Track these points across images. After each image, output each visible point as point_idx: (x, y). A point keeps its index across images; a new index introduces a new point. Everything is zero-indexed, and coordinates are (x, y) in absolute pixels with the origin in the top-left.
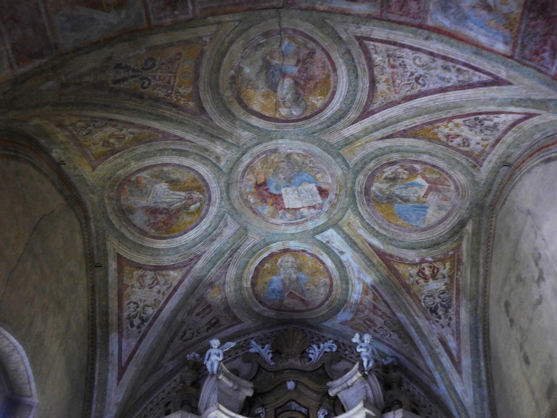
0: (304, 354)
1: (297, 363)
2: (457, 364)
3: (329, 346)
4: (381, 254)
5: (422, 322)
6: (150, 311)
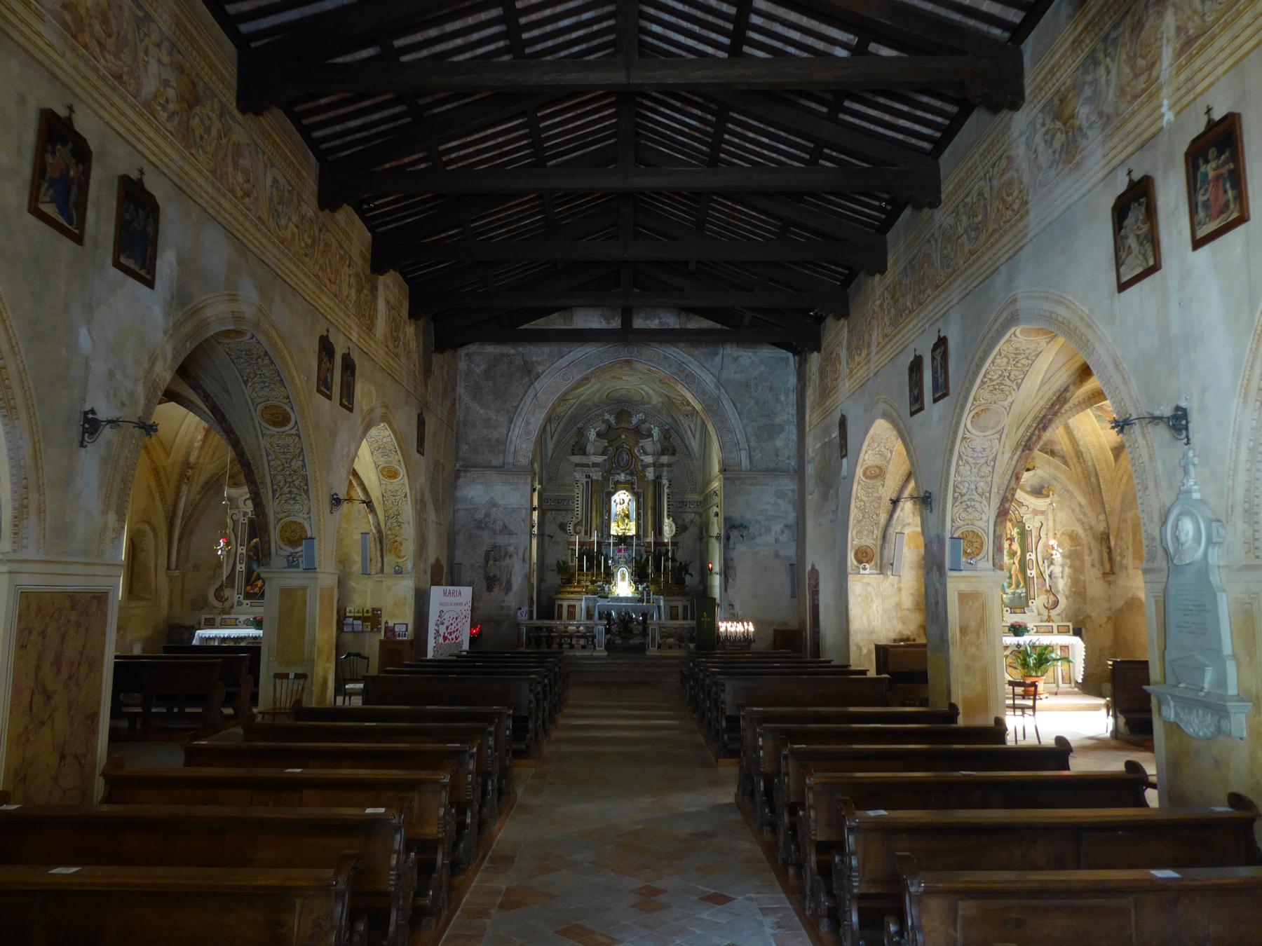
1: (626, 426)
2: (694, 436)
3: (641, 416)
4: (667, 396)
5: (681, 418)
6: (563, 414)
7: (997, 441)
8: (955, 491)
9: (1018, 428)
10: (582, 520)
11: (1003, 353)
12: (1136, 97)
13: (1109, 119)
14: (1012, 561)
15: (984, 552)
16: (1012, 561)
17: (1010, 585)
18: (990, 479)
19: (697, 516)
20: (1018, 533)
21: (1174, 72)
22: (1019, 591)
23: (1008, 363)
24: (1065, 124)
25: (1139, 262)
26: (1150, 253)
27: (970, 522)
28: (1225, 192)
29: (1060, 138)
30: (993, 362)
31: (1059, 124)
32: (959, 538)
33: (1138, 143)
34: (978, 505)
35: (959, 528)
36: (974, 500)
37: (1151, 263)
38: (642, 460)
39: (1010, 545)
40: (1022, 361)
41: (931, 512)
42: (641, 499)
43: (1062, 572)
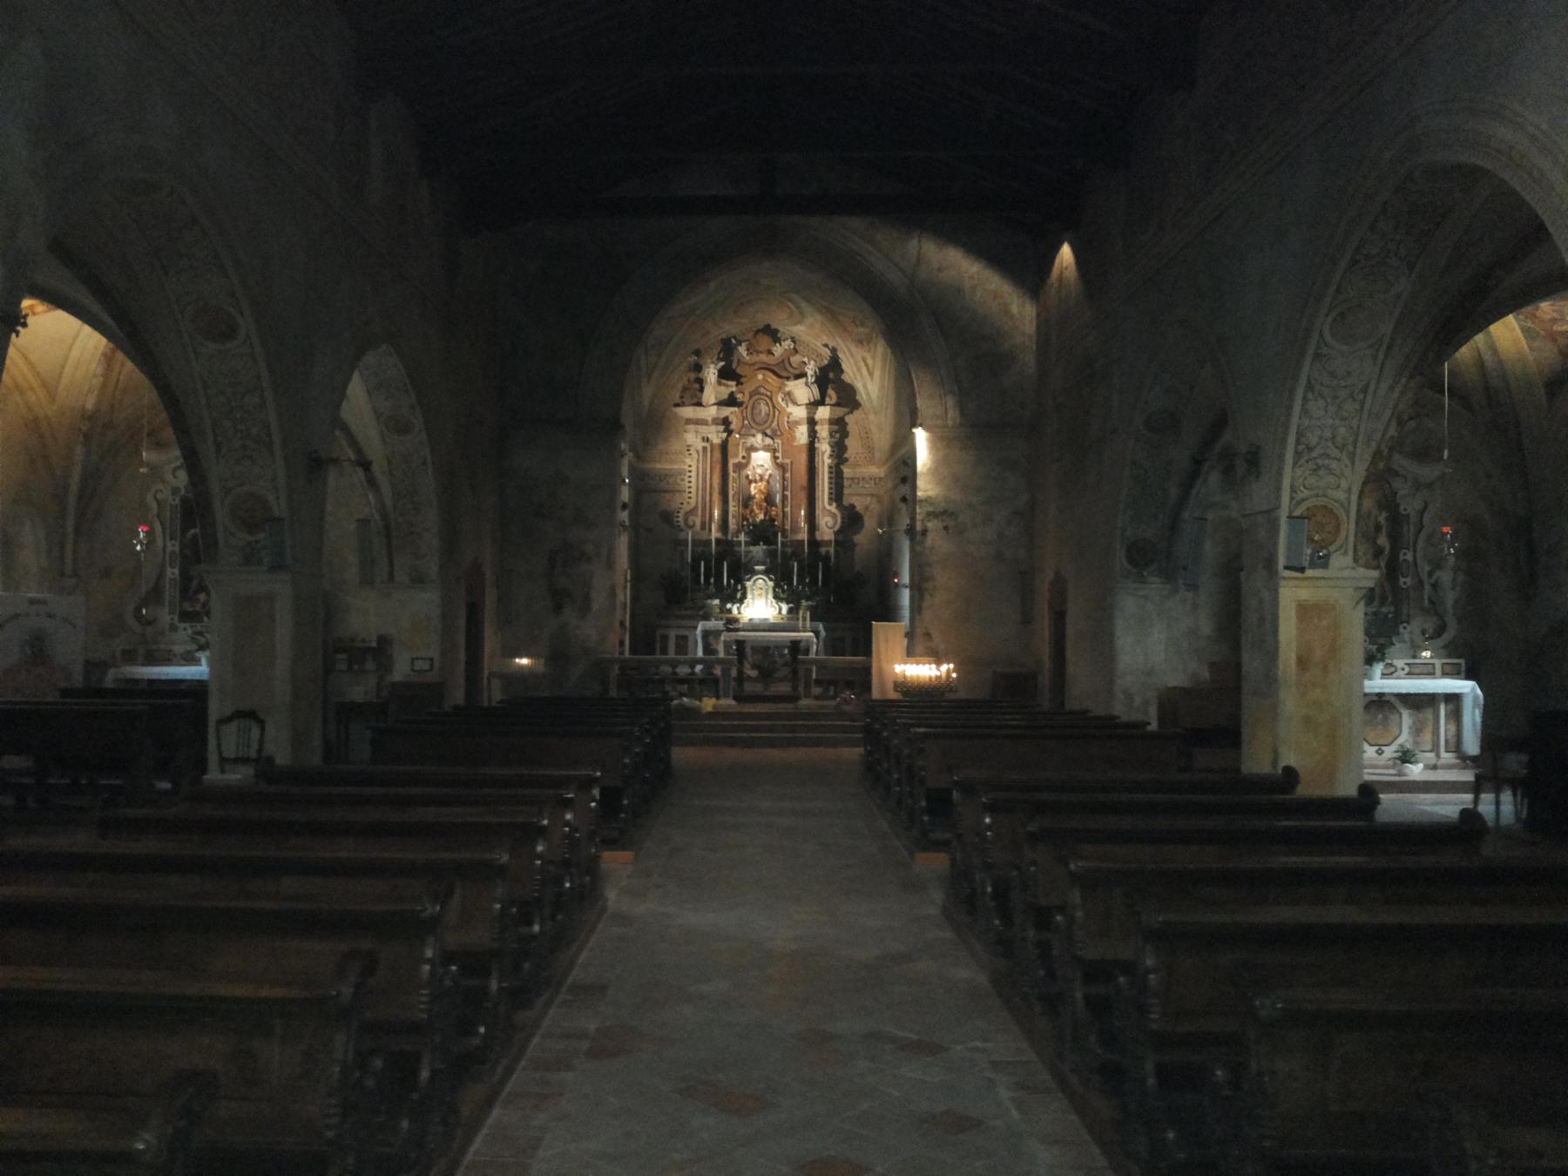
0: (770, 352)
2: (871, 374)
3: (788, 344)
8: (1298, 442)
10: (696, 507)
19: (875, 500)
20: (1387, 519)
27: (1321, 493)
32: (1302, 517)
34: (1334, 465)
35: (1303, 500)
36: (1328, 456)
38: (789, 415)
41: (1258, 477)
42: (788, 475)
43: (1454, 580)
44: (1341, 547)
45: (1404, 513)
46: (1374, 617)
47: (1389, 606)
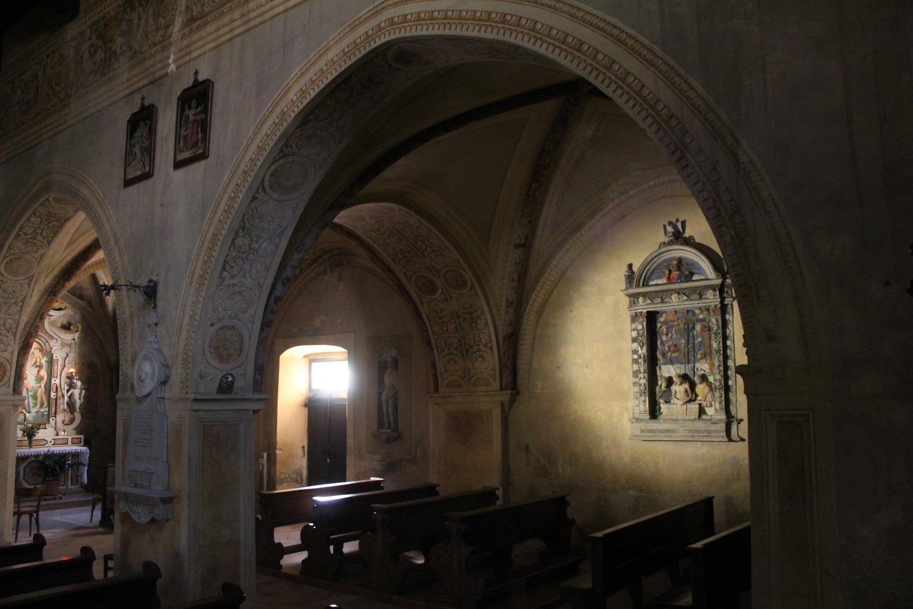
7: (26, 285)
9: (47, 276)
11: (38, 214)
12: (155, 45)
13: (135, 53)
14: (38, 385)
15: (6, 379)
16: (38, 385)
17: (36, 405)
18: (17, 317)
20: (47, 362)
21: (180, 37)
22: (42, 410)
23: (41, 222)
24: (105, 45)
25: (140, 167)
26: (147, 162)
28: (198, 133)
29: (100, 55)
30: (28, 219)
31: (101, 43)
33: (151, 78)
37: (147, 170)
39: (39, 371)
40: (54, 223)
44: (6, 384)
45: (56, 358)
46: (36, 414)
47: (45, 407)
